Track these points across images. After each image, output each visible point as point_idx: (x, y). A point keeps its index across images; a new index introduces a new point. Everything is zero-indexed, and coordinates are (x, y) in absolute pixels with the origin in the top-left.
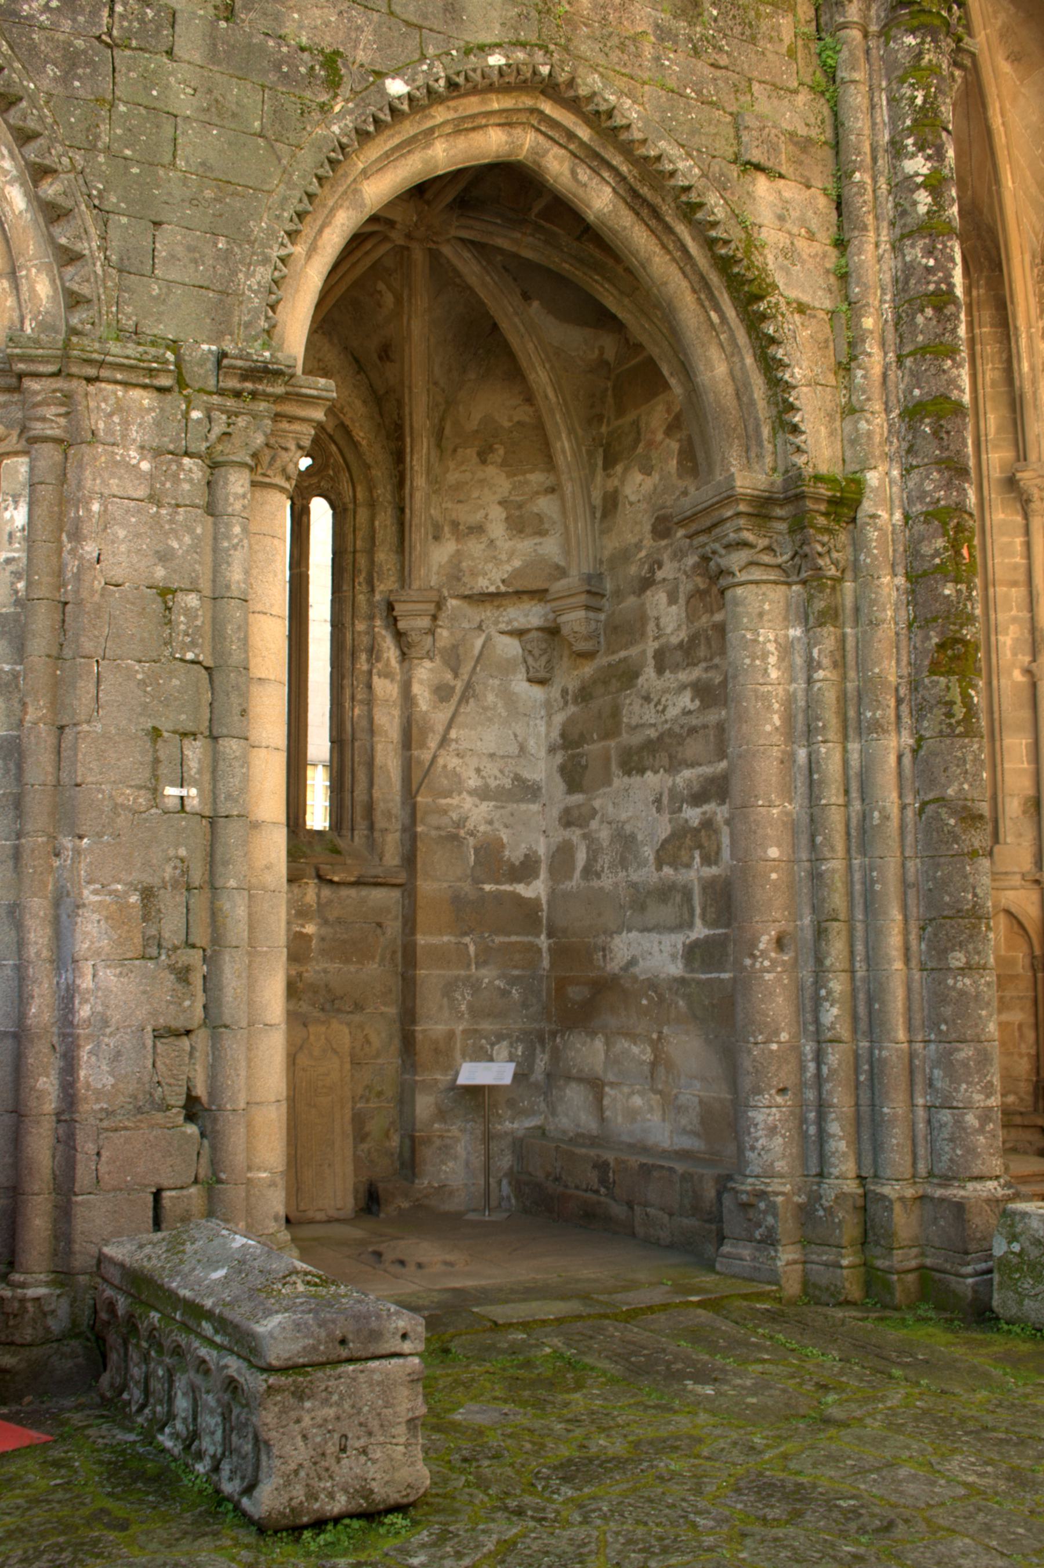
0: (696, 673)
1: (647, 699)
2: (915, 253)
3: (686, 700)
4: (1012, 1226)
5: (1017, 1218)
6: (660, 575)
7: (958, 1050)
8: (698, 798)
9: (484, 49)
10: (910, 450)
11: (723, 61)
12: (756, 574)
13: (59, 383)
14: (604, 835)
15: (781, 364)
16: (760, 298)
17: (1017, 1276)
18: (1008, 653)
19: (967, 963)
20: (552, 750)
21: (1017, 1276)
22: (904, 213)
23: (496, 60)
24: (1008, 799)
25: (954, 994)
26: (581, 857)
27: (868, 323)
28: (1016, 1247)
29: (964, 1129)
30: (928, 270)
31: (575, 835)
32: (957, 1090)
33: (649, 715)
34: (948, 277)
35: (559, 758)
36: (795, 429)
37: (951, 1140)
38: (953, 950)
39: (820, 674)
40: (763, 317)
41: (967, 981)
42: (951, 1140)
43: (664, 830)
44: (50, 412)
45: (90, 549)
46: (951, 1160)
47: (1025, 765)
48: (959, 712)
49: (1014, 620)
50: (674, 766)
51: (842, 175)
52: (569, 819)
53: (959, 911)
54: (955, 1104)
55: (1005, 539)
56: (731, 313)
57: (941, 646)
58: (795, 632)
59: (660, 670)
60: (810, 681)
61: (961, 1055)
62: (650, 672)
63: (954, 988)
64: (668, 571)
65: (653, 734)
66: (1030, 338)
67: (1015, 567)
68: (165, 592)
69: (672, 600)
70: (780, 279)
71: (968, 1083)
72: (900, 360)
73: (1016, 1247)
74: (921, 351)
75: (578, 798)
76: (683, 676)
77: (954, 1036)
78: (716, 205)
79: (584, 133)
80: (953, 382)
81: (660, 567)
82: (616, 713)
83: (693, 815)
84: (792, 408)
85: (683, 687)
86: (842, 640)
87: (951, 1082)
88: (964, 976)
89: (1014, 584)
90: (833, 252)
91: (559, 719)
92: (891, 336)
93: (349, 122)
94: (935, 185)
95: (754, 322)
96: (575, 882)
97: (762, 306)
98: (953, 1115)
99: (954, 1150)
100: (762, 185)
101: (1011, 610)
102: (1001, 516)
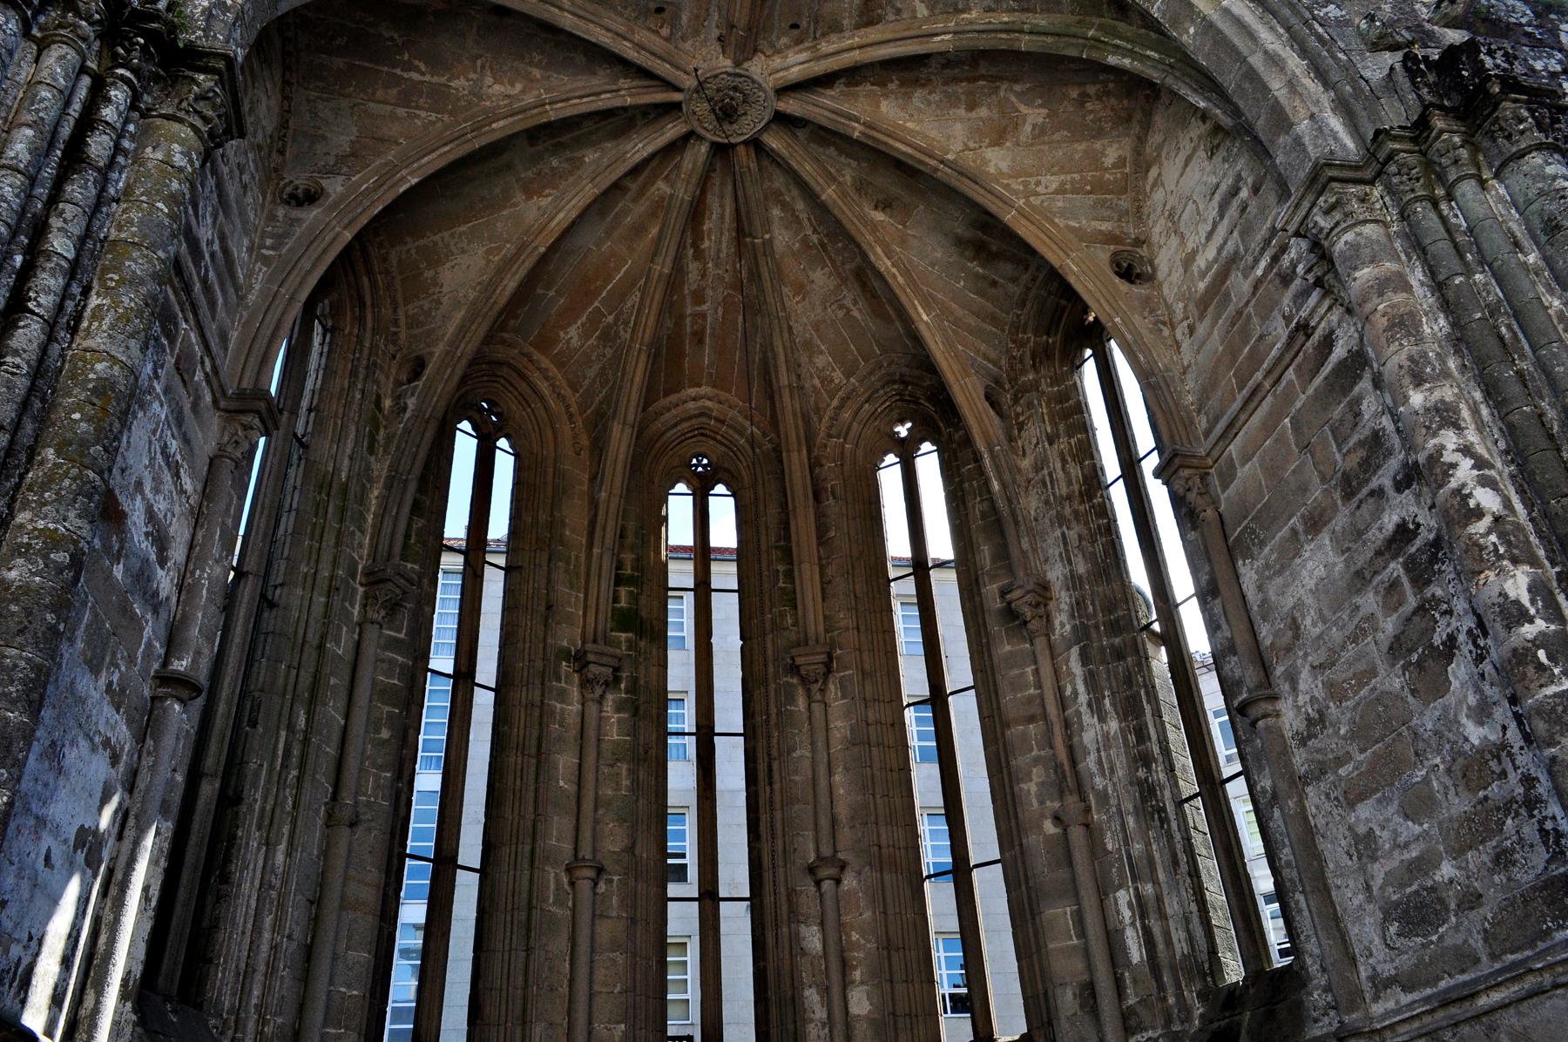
18: (1035, 802)
24: (1059, 991)
47: (1075, 941)
49: (1037, 761)
55: (1016, 672)
66: (993, 456)
67: (1030, 700)
89: (1031, 719)
101: (1032, 750)
102: (1008, 648)
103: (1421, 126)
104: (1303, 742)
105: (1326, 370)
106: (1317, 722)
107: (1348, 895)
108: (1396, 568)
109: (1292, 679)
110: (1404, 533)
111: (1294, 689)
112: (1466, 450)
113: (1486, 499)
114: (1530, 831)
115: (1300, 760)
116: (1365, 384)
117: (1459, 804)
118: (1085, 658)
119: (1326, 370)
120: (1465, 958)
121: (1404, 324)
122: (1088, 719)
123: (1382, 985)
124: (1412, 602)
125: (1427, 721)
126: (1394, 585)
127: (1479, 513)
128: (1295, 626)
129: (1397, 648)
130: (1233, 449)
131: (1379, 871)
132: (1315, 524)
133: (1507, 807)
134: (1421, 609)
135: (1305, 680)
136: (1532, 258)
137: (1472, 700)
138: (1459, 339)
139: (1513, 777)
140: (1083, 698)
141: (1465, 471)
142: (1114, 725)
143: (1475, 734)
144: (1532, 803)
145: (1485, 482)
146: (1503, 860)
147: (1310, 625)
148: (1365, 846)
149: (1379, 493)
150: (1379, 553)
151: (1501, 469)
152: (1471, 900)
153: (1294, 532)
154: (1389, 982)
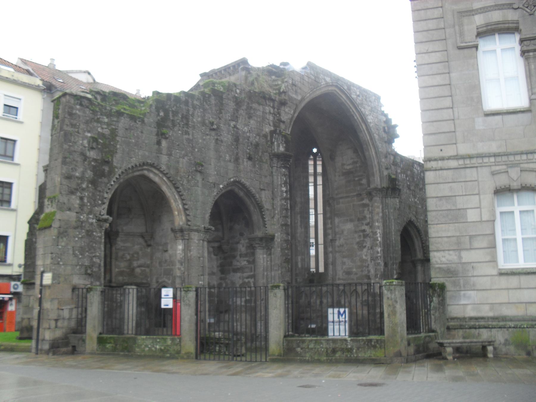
0: (247, 259)
1: (238, 261)
2: (283, 202)
3: (245, 263)
6: (241, 242)
8: (247, 278)
9: (230, 179)
10: (282, 231)
11: (258, 173)
12: (259, 248)
13: (188, 232)
14: (229, 282)
15: (265, 218)
16: (262, 209)
20: (218, 267)
22: (282, 196)
23: (232, 180)
26: (224, 285)
27: (276, 212)
30: (285, 205)
31: (223, 281)
33: (238, 264)
34: (287, 206)
35: (219, 268)
36: (266, 227)
39: (268, 262)
40: (263, 211)
43: (241, 282)
44: (187, 235)
45: (192, 253)
48: (287, 268)
50: (243, 272)
51: (273, 189)
52: (221, 279)
56: (258, 210)
57: (285, 259)
58: (265, 256)
59: (240, 257)
60: (267, 263)
62: (238, 257)
64: (242, 241)
65: (239, 267)
68: (199, 258)
69: (243, 246)
70: (265, 206)
72: (280, 217)
74: (284, 217)
75: (223, 276)
76: (244, 259)
78: (257, 196)
79: (241, 186)
80: (288, 222)
81: (241, 240)
82: (232, 262)
83: (246, 280)
84: (266, 224)
85: (245, 260)
86: (271, 257)
90: (272, 200)
91: (219, 262)
92: (279, 213)
93: (216, 193)
94: (286, 192)
95: (261, 212)
96: (222, 290)
97: (263, 210)
100: (263, 192)
103: (388, 188)
104: (338, 247)
105: (361, 202)
106: (342, 246)
107: (339, 268)
108: (361, 234)
109: (340, 238)
110: (364, 231)
111: (340, 239)
112: (379, 233)
113: (379, 239)
114: (367, 270)
115: (337, 249)
116: (366, 209)
117: (359, 264)
118: (301, 217)
119: (361, 202)
120: (353, 279)
121: (378, 214)
122: (299, 227)
123: (339, 279)
124: (362, 239)
125: (359, 253)
126: (360, 236)
127: (378, 240)
128: (343, 232)
129: (358, 243)
130: (341, 200)
131: (344, 267)
132: (351, 221)
133: (365, 266)
134: (363, 241)
135: (342, 240)
136: (392, 211)
137: (365, 254)
138: (383, 217)
139: (367, 264)
140: (299, 224)
141: (379, 235)
142: (303, 230)
143: (364, 257)
144: (368, 267)
145: (380, 237)
146: (362, 271)
147: (345, 233)
148: (344, 263)
149: (363, 224)
150: (360, 231)
151: (381, 236)
152: (356, 274)
153: (347, 220)
154: (341, 279)
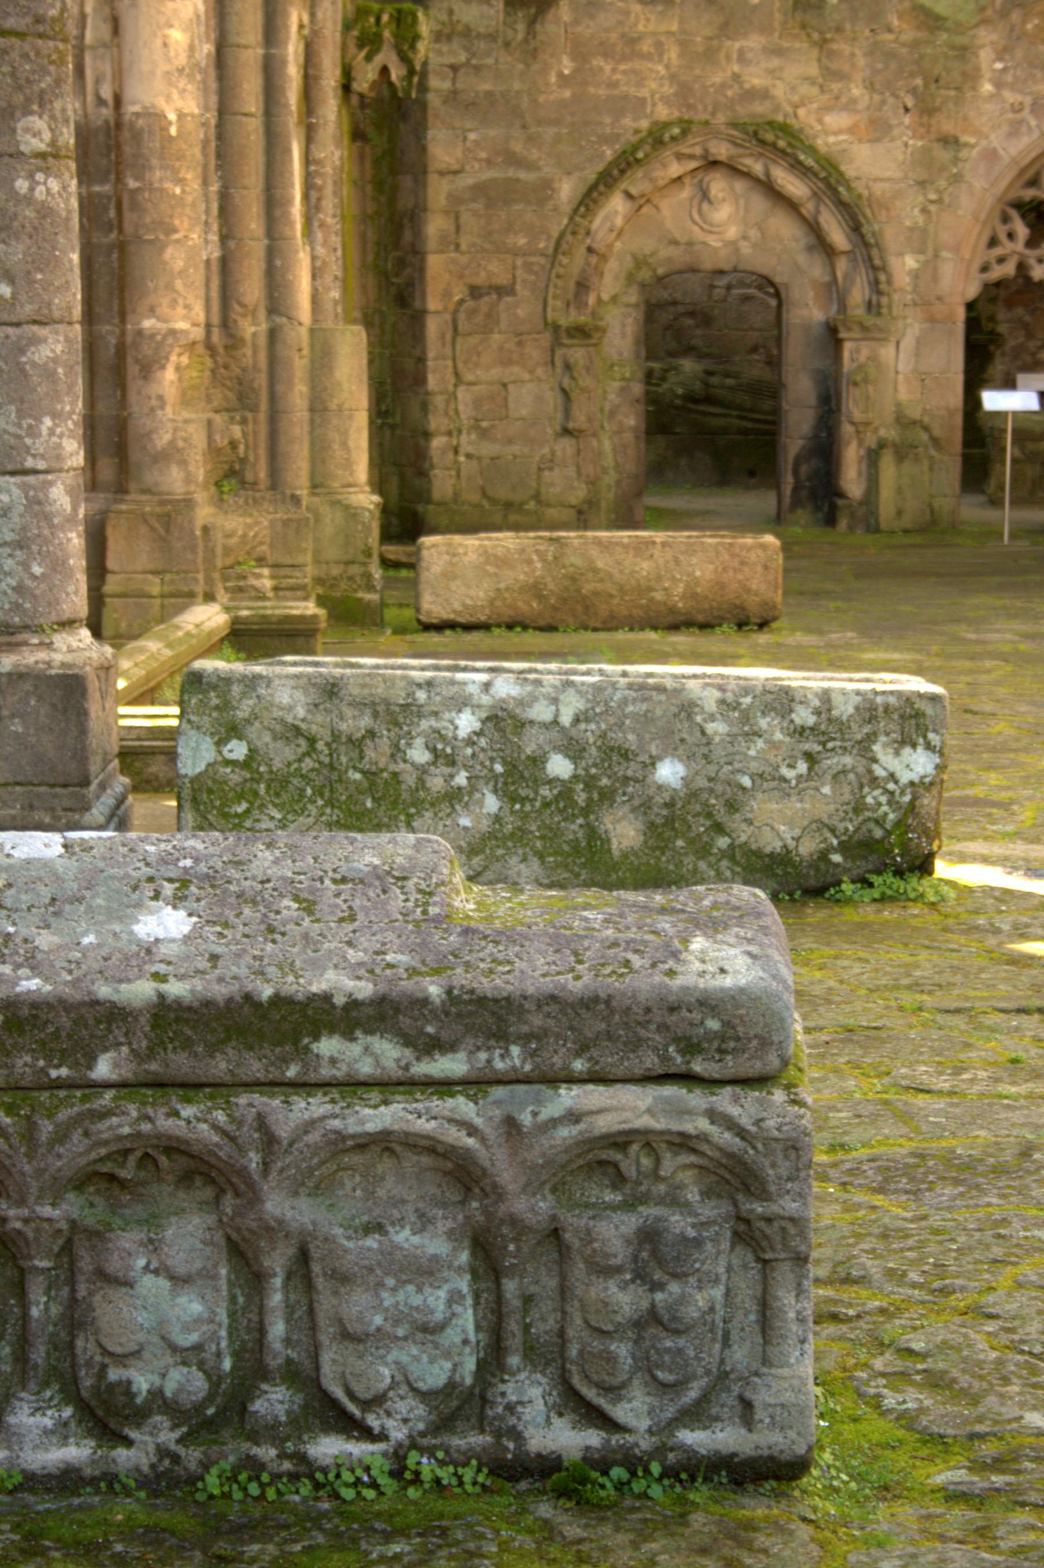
4: (225, 706)
5: (236, 689)
7: (35, 341)
17: (240, 809)
19: (53, 143)
21: (240, 809)
25: (30, 213)
28: (237, 750)
29: (47, 517)
32: (33, 432)
37: (20, 545)
38: (29, 113)
41: (54, 185)
42: (20, 545)
46: (19, 589)
53: (39, 20)
54: (30, 463)
61: (43, 353)
63: (29, 199)
71: (55, 415)
73: (237, 750)
77: (28, 309)
87: (21, 414)
88: (47, 171)
98: (25, 488)
99: (26, 566)
